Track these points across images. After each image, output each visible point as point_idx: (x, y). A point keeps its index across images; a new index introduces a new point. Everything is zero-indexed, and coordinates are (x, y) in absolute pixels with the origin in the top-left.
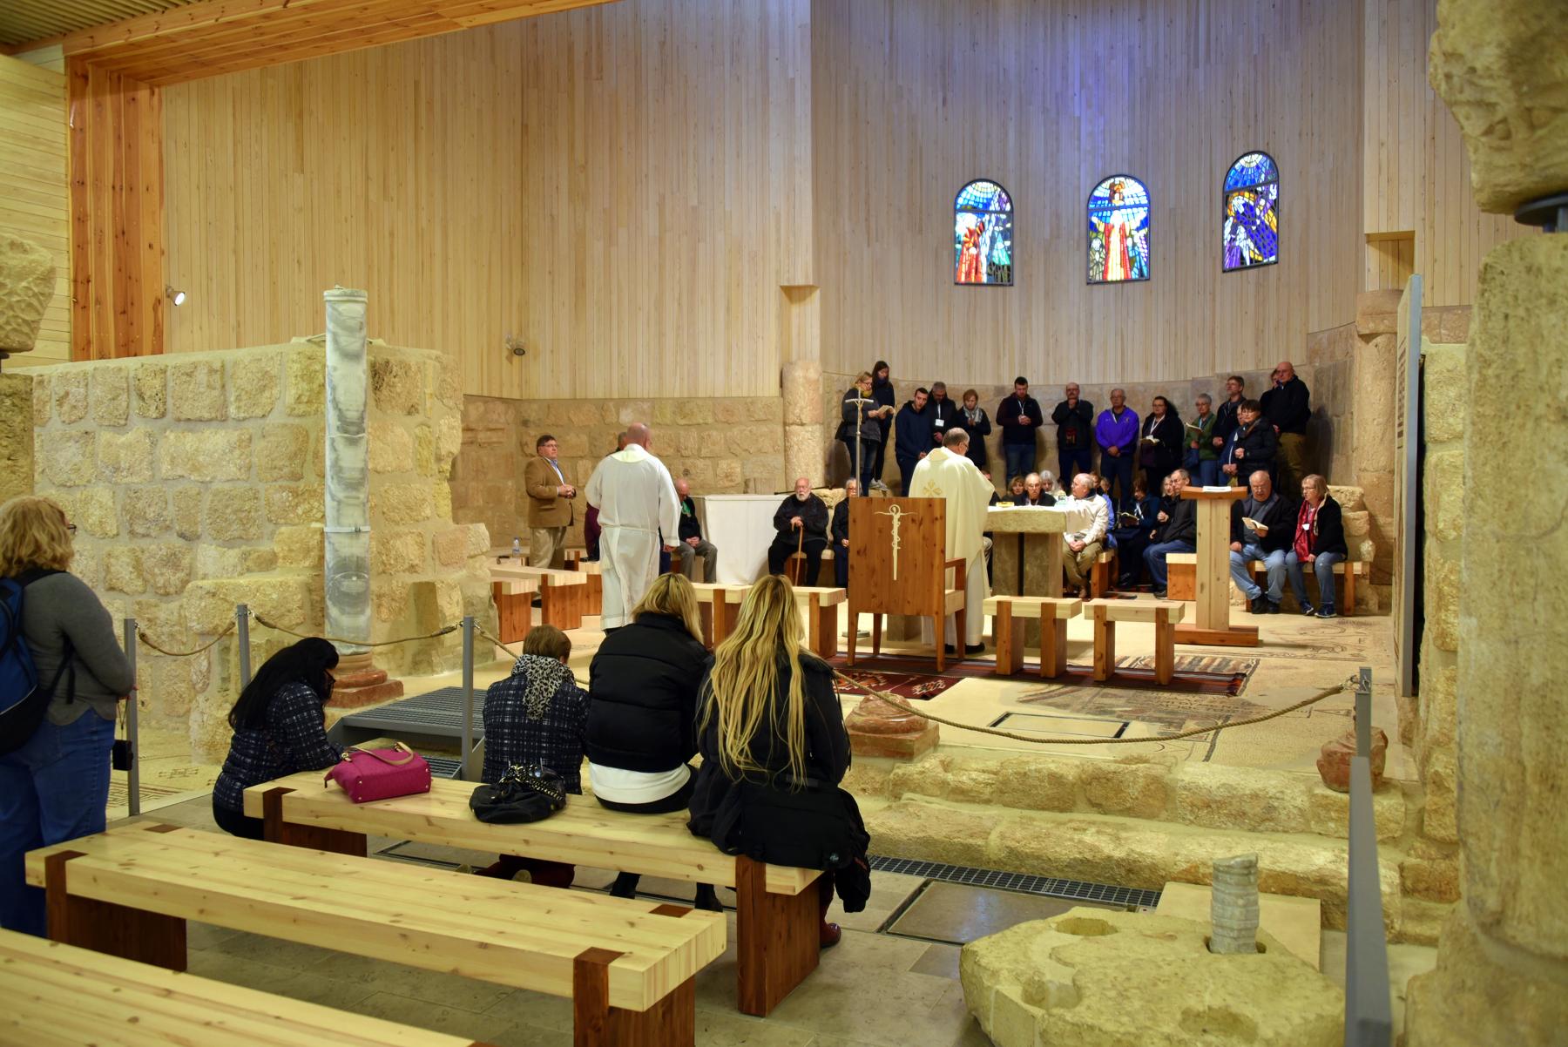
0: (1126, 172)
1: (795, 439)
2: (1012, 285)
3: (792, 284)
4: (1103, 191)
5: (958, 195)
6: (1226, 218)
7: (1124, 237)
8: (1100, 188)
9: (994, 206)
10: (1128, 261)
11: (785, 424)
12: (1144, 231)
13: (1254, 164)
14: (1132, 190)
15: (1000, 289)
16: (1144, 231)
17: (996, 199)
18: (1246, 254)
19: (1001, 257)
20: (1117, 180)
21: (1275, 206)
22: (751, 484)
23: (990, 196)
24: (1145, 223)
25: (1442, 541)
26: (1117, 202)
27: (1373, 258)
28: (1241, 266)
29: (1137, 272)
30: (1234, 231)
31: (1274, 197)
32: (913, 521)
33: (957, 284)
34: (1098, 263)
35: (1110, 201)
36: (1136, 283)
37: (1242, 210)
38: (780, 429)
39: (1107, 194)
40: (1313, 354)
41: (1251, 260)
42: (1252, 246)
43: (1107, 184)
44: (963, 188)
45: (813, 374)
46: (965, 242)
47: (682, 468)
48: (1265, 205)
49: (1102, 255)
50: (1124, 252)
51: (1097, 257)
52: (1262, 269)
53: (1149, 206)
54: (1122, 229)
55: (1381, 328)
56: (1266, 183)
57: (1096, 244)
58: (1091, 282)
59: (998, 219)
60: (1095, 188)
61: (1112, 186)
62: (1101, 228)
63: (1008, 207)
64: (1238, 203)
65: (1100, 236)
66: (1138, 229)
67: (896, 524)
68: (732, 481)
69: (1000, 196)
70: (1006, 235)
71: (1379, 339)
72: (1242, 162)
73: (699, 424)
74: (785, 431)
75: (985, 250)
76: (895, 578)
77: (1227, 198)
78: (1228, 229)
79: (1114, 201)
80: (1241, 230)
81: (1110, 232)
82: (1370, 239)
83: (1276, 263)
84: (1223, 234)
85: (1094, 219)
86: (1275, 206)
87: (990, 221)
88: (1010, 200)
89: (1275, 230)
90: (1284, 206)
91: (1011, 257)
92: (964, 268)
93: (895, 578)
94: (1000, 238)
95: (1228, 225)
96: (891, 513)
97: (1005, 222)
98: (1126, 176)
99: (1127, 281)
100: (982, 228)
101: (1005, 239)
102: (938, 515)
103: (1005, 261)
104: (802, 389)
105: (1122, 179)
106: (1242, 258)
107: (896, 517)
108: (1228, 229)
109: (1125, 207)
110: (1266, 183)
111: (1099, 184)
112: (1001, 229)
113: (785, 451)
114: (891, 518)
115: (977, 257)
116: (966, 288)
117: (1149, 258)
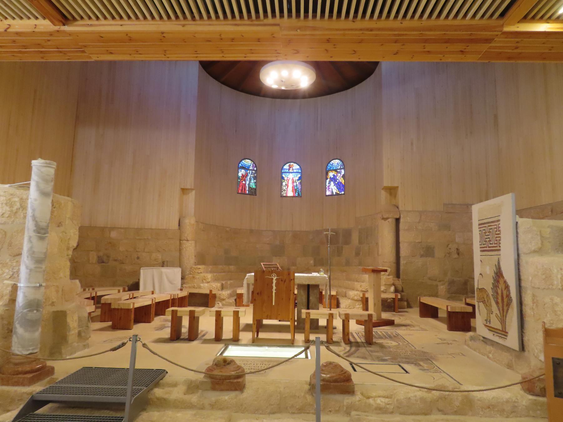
0: (294, 161)
1: (185, 246)
2: (256, 195)
3: (185, 187)
4: (286, 167)
6: (327, 179)
7: (293, 182)
8: (285, 166)
9: (251, 168)
10: (295, 190)
11: (180, 240)
12: (299, 181)
13: (336, 163)
14: (296, 167)
15: (252, 196)
16: (299, 181)
17: (252, 166)
19: (253, 185)
20: (291, 164)
21: (344, 176)
22: (166, 263)
23: (250, 164)
26: (291, 171)
27: (383, 195)
29: (297, 194)
31: (343, 173)
32: (282, 280)
33: (238, 193)
34: (284, 190)
35: (289, 170)
36: (297, 198)
37: (332, 177)
38: (178, 242)
39: (288, 168)
41: (336, 193)
42: (336, 188)
43: (288, 165)
44: (241, 161)
45: (193, 221)
46: (242, 179)
47: (136, 256)
48: (340, 176)
49: (286, 188)
50: (293, 187)
51: (284, 188)
52: (339, 196)
53: (301, 173)
54: (293, 179)
55: (390, 216)
56: (340, 169)
57: (284, 184)
60: (284, 165)
61: (289, 166)
62: (286, 179)
63: (255, 169)
64: (331, 174)
65: (285, 181)
66: (298, 180)
67: (274, 282)
68: (157, 262)
69: (253, 165)
70: (255, 178)
71: (389, 220)
72: (332, 161)
73: (145, 239)
74: (180, 243)
75: (248, 182)
76: (274, 304)
77: (327, 172)
79: (290, 170)
80: (332, 183)
81: (288, 180)
83: (344, 194)
84: (326, 184)
85: (284, 176)
86: (344, 176)
87: (249, 173)
88: (256, 167)
89: (344, 184)
91: (256, 185)
93: (274, 304)
94: (252, 179)
96: (273, 277)
97: (254, 174)
98: (294, 163)
99: (294, 197)
100: (247, 175)
101: (254, 179)
102: (292, 279)
103: (254, 187)
104: (188, 227)
105: (293, 163)
106: (332, 192)
107: (275, 278)
108: (327, 183)
109: (294, 172)
110: (340, 169)
111: (285, 164)
112: (253, 176)
114: (272, 279)
115: (245, 184)
116: (241, 195)
117: (301, 189)
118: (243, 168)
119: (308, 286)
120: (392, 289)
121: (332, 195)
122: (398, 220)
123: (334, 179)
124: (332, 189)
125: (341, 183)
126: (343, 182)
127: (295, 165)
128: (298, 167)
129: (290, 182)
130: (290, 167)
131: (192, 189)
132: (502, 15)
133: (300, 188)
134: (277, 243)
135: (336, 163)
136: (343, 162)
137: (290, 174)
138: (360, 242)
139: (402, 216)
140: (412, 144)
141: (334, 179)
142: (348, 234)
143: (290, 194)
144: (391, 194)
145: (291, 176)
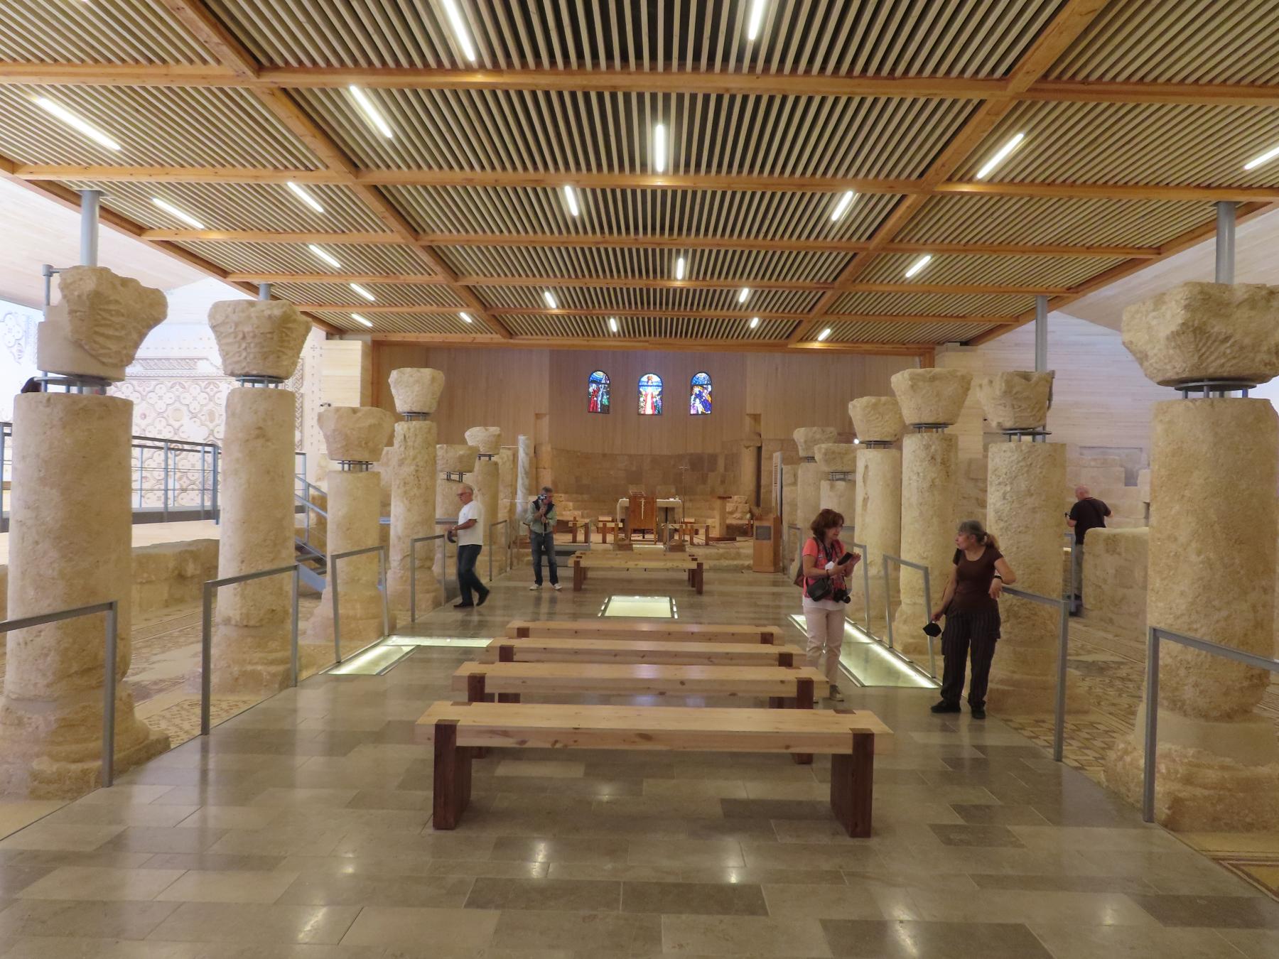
4: (644, 379)
7: (652, 398)
9: (603, 381)
10: (654, 407)
14: (655, 379)
19: (605, 401)
20: (650, 375)
21: (710, 393)
24: (660, 393)
26: (650, 384)
27: (748, 420)
30: (694, 400)
43: (646, 376)
45: (549, 448)
50: (653, 403)
57: (642, 399)
58: (639, 414)
62: (644, 393)
64: (697, 390)
70: (608, 393)
71: (751, 448)
75: (600, 399)
80: (698, 400)
86: (710, 393)
91: (609, 402)
95: (693, 397)
103: (607, 403)
110: (707, 384)
119: (667, 508)
120: (748, 516)
121: (697, 414)
122: (759, 449)
124: (698, 407)
126: (710, 399)
128: (659, 379)
130: (649, 379)
131: (545, 415)
132: (788, 337)
133: (660, 404)
134: (634, 468)
138: (726, 470)
140: (777, 369)
141: (699, 396)
142: (713, 458)
143: (649, 411)
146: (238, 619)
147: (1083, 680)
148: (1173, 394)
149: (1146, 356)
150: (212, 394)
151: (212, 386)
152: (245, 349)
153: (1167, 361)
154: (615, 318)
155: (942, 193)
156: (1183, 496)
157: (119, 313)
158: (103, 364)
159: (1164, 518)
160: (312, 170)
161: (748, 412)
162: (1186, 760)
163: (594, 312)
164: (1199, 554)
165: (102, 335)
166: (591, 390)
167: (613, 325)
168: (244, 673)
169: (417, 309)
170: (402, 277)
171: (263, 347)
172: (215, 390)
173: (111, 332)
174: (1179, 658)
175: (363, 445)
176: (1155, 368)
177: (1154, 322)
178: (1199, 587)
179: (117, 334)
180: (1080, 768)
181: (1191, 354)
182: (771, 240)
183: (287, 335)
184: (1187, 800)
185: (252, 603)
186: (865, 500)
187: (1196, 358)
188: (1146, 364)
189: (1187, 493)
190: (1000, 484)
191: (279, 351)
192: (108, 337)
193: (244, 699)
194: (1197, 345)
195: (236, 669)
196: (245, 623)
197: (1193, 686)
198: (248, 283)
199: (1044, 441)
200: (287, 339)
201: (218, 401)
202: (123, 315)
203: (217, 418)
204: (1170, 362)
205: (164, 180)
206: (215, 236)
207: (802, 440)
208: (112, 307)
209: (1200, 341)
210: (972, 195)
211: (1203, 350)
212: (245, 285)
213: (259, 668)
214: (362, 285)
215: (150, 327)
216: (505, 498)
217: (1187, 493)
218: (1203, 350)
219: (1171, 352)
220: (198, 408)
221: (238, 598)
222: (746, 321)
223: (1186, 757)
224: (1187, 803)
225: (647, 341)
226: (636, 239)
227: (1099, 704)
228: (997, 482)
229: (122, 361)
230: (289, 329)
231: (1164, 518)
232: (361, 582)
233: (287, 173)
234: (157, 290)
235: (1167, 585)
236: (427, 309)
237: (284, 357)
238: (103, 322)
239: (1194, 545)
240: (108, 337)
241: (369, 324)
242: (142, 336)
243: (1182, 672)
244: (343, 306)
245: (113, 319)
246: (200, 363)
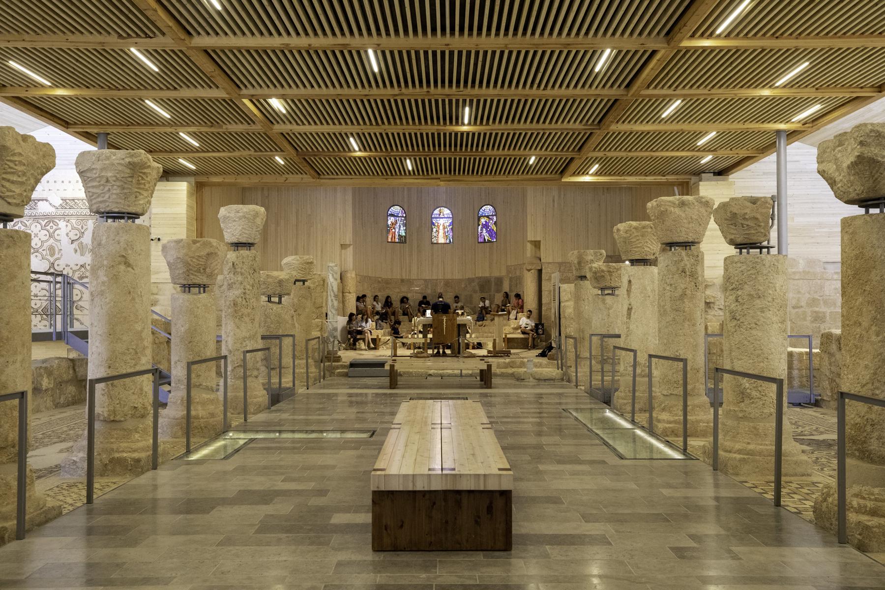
0: (444, 205)
4: (437, 212)
5: (388, 210)
6: (479, 225)
7: (444, 228)
11: (343, 293)
12: (451, 227)
14: (446, 212)
18: (486, 238)
21: (495, 223)
25: (565, 317)
26: (441, 216)
27: (529, 246)
28: (484, 241)
37: (484, 223)
40: (508, 272)
43: (438, 209)
44: (390, 208)
45: (353, 276)
50: (445, 233)
53: (453, 218)
54: (444, 225)
56: (492, 215)
57: (434, 230)
58: (432, 243)
59: (401, 219)
60: (434, 210)
62: (436, 225)
63: (405, 215)
64: (483, 220)
66: (449, 226)
70: (405, 225)
75: (397, 230)
78: (479, 229)
82: (528, 241)
85: (434, 221)
86: (495, 223)
88: (405, 213)
90: (498, 224)
91: (405, 233)
92: (390, 237)
95: (480, 227)
98: (445, 207)
100: (396, 223)
103: (404, 234)
106: (485, 239)
108: (479, 229)
109: (445, 218)
110: (492, 215)
113: (343, 302)
115: (395, 232)
118: (392, 215)
122: (540, 271)
123: (486, 226)
125: (493, 230)
127: (446, 209)
128: (448, 212)
129: (441, 227)
131: (350, 245)
132: (562, 172)
135: (488, 209)
136: (494, 209)
137: (441, 220)
139: (543, 268)
140: (554, 201)
141: (486, 226)
143: (442, 240)
144: (536, 246)
145: (441, 221)
146: (106, 415)
147: (812, 453)
148: (857, 211)
149: (835, 181)
150: (51, 231)
151: (51, 224)
152: (109, 190)
153: (849, 185)
154: (410, 159)
155: (686, 47)
156: (864, 290)
157: (20, 162)
158: (9, 203)
159: (851, 308)
160: (151, 38)
161: (528, 239)
162: (873, 497)
163: (392, 154)
164: (878, 335)
165: (8, 181)
166: (389, 223)
167: (409, 165)
168: (112, 460)
169: (236, 154)
170: (224, 127)
171: (124, 189)
172: (55, 227)
173: (15, 178)
174: (865, 418)
175: (202, 271)
176: (841, 191)
177: (839, 155)
178: (879, 361)
179: (19, 179)
180: (800, 513)
181: (867, 179)
182: (544, 89)
183: (143, 179)
184: (873, 527)
185: (118, 402)
186: (630, 309)
187: (871, 181)
188: (835, 188)
189: (868, 288)
190: (733, 289)
191: (136, 192)
192: (13, 182)
193: (114, 481)
194: (871, 173)
195: (104, 456)
196: (112, 418)
197: (877, 439)
198: (87, 132)
199: (768, 253)
200: (143, 182)
201: (57, 237)
202: (24, 165)
203: (57, 252)
204: (852, 185)
205: (20, 45)
206: (60, 92)
207: (576, 262)
208: (16, 158)
209: (874, 168)
210: (712, 49)
211: (876, 176)
212: (84, 134)
213: (125, 455)
214: (189, 133)
215: (43, 174)
216: (317, 318)
217: (868, 288)
218: (876, 176)
219: (852, 178)
220: (39, 244)
221: (106, 397)
222: (525, 159)
223: (873, 494)
224: (874, 529)
225: (439, 179)
226: (428, 92)
227: (822, 469)
228: (730, 288)
229: (23, 201)
230: (144, 173)
231: (851, 308)
232: (201, 387)
233: (130, 40)
234: (48, 144)
235: (855, 360)
236: (246, 153)
237: (142, 197)
238: (9, 170)
239: (874, 328)
240: (13, 182)
241: (193, 167)
242: (38, 181)
243: (869, 428)
244: (171, 152)
245: (16, 168)
246: (40, 204)
